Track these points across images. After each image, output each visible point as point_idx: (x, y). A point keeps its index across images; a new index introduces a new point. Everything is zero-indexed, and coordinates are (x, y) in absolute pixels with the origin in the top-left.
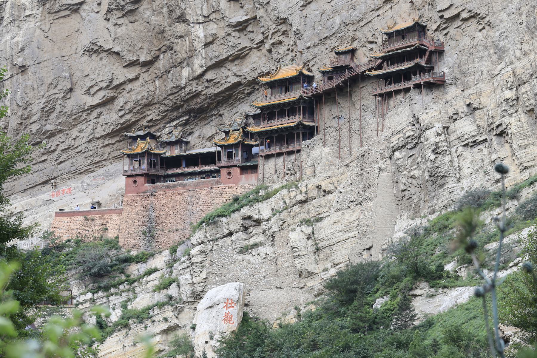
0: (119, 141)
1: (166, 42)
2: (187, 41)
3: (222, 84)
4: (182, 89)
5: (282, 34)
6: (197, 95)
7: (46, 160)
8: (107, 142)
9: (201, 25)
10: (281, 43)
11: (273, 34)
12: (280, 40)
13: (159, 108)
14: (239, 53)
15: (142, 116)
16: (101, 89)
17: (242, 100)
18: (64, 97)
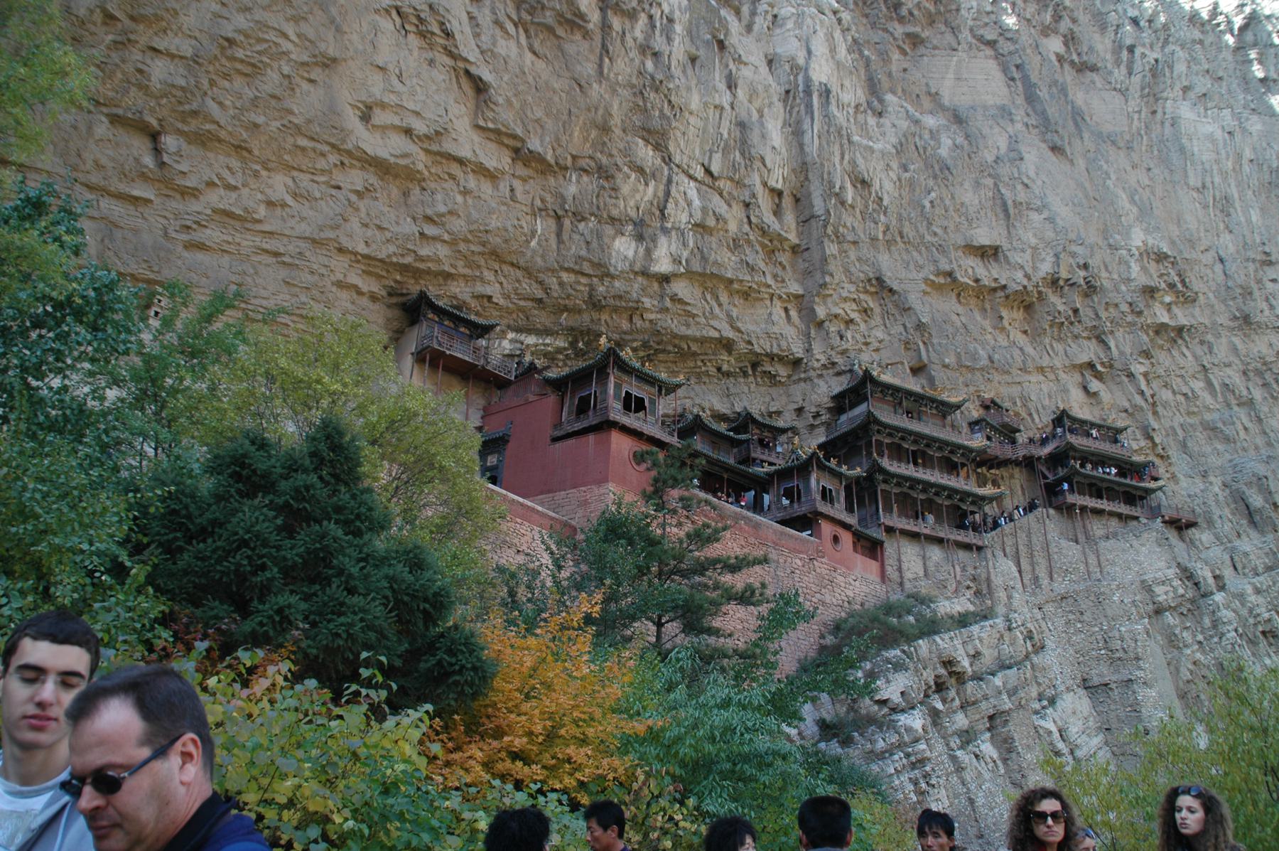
0: (373, 298)
1: (599, 155)
2: (651, 190)
3: (698, 323)
4: (608, 275)
5: (859, 311)
6: (634, 311)
7: (148, 201)
8: (354, 279)
9: (692, 184)
10: (850, 322)
11: (845, 300)
12: (854, 315)
13: (518, 281)
14: (755, 286)
15: (467, 271)
16: (408, 132)
17: (705, 379)
18: (303, 64)
